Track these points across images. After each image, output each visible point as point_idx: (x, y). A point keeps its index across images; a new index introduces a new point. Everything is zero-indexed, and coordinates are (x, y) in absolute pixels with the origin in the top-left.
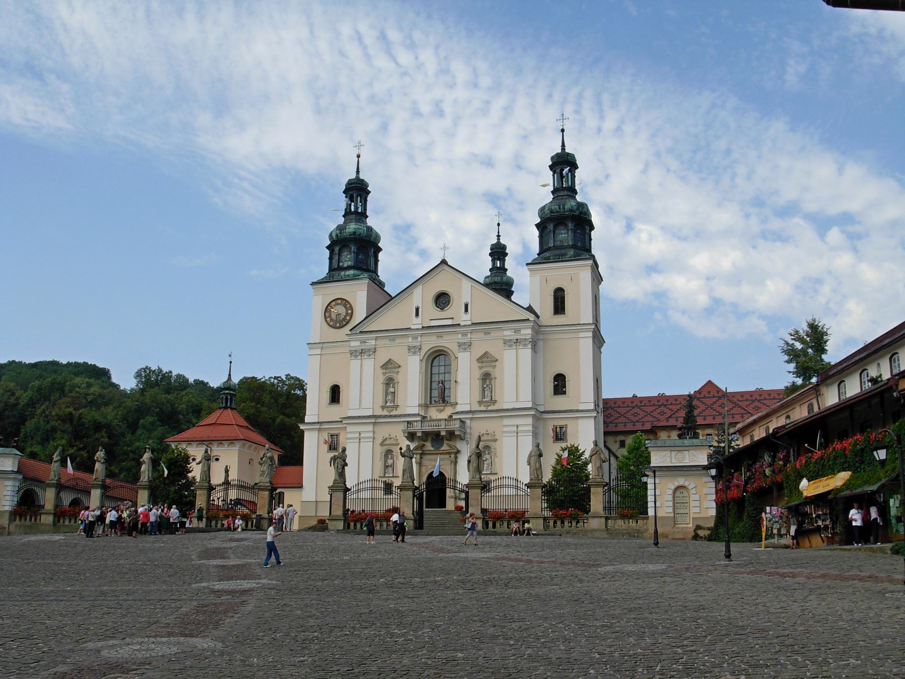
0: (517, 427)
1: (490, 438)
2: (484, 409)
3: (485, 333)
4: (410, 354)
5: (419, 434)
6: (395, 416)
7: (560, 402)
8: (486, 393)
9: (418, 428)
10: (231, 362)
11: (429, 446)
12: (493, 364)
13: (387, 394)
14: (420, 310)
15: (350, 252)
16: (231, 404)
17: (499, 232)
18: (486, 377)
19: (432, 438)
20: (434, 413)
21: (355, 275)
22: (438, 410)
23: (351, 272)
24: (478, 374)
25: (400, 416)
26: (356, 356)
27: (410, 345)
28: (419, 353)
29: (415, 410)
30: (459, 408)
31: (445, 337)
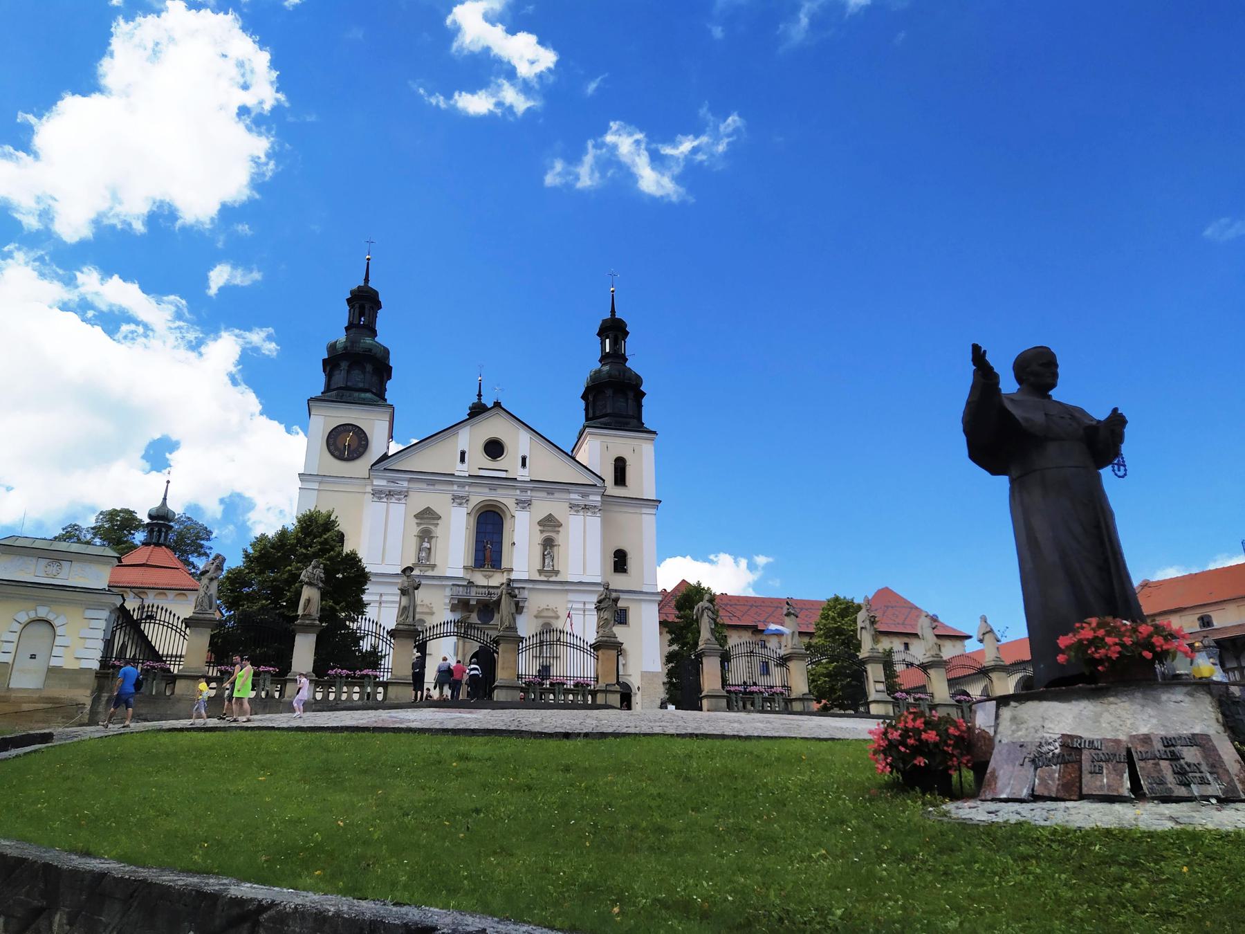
0: (584, 603)
1: (551, 614)
2: (546, 579)
3: (548, 493)
4: (455, 505)
5: (473, 602)
6: (433, 578)
7: (618, 582)
8: (547, 561)
9: (474, 596)
10: (168, 482)
11: (474, 618)
12: (557, 529)
13: (420, 550)
14: (466, 455)
15: (364, 372)
16: (166, 538)
17: (480, 392)
18: (548, 544)
19: (479, 608)
20: (480, 579)
21: (371, 400)
22: (485, 576)
23: (368, 395)
24: (539, 538)
25: (440, 578)
26: (380, 498)
27: (456, 494)
28: (465, 505)
29: (460, 573)
30: (514, 576)
31: (500, 491)
